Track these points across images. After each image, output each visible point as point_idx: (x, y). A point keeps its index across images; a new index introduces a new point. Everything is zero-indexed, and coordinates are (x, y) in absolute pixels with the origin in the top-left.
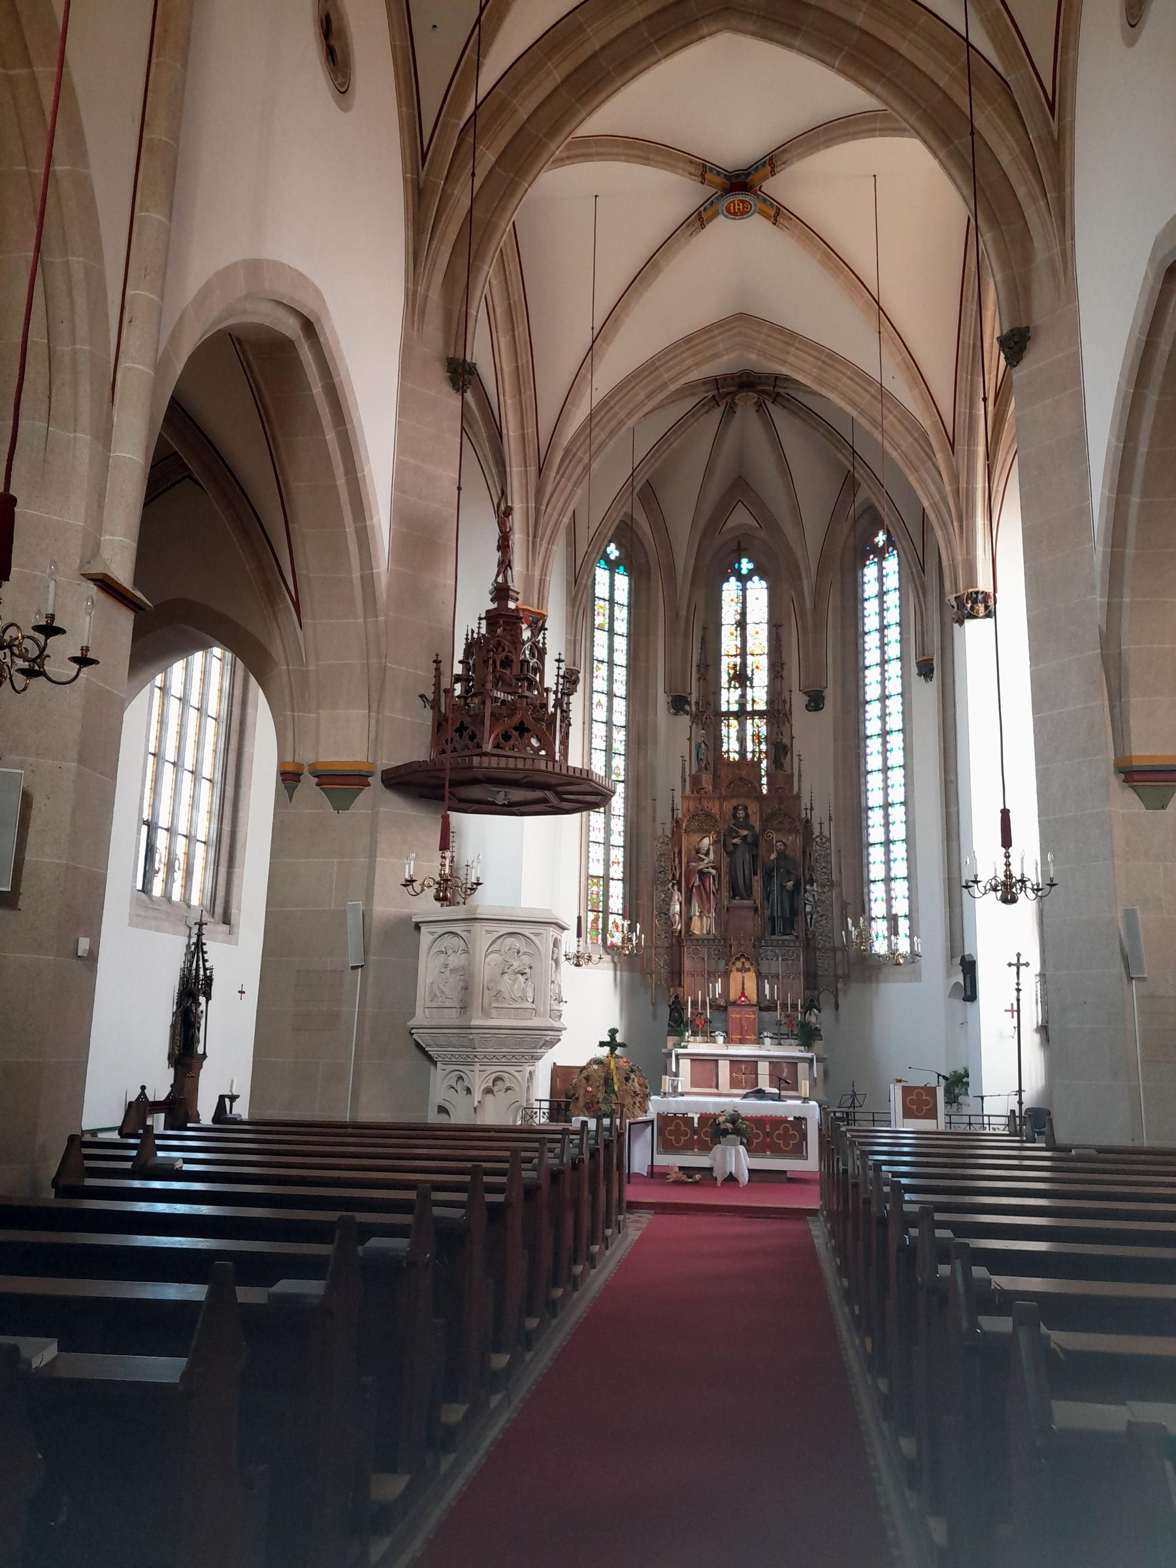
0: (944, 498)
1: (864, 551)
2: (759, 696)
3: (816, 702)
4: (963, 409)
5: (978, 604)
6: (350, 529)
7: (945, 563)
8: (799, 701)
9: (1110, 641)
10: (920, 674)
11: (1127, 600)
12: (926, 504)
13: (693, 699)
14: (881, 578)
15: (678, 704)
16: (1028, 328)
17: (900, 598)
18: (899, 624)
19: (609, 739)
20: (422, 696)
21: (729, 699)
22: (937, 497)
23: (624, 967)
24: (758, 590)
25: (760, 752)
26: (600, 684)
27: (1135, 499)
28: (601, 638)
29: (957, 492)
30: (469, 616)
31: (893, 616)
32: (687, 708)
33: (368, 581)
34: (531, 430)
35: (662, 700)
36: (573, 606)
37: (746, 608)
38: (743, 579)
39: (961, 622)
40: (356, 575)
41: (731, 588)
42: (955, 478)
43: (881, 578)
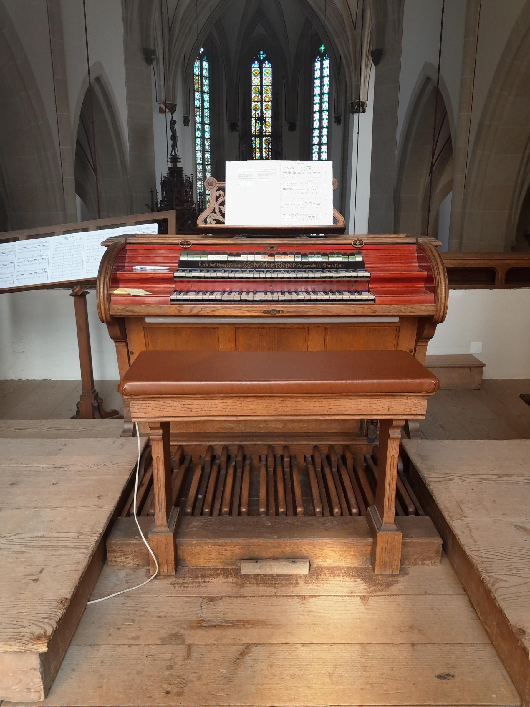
0: (349, 53)
1: (315, 55)
2: (269, 129)
3: (292, 127)
4: (360, 9)
5: (360, 107)
6: (115, 145)
7: (348, 84)
8: (285, 126)
9: (397, 191)
10: (335, 122)
11: (404, 179)
12: (342, 55)
13: (239, 124)
14: (322, 69)
15: (233, 127)
16: (382, 49)
17: (329, 81)
18: (328, 127)
19: (203, 145)
20: (147, 205)
21: (255, 127)
22: (347, 53)
23: (289, 545)
24: (267, 68)
25: (269, 148)
26: (198, 119)
27: (410, 146)
28: (197, 95)
29: (355, 51)
30: (161, 170)
31: (326, 89)
32: (237, 128)
33: (123, 162)
34: (164, 11)
35: (226, 124)
36: (185, 84)
37: (262, 77)
38: (261, 63)
39: (353, 114)
40: (119, 162)
41: (255, 66)
42: (355, 44)
43: (322, 69)
